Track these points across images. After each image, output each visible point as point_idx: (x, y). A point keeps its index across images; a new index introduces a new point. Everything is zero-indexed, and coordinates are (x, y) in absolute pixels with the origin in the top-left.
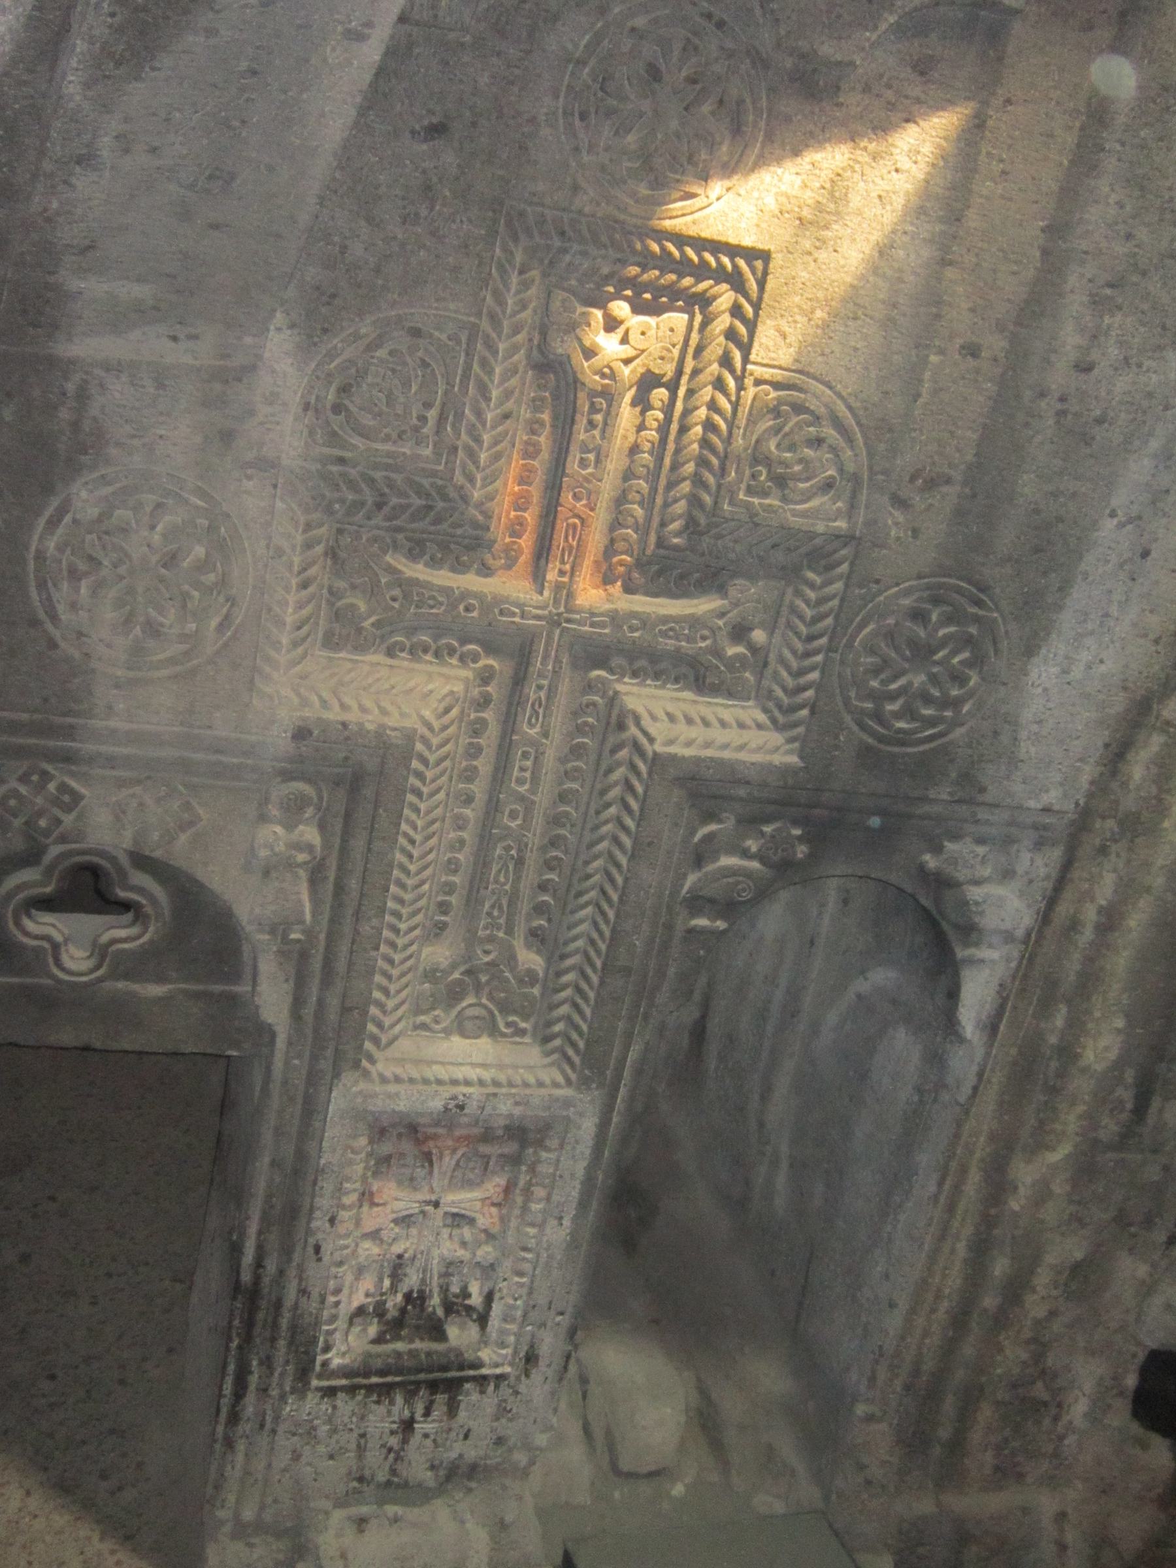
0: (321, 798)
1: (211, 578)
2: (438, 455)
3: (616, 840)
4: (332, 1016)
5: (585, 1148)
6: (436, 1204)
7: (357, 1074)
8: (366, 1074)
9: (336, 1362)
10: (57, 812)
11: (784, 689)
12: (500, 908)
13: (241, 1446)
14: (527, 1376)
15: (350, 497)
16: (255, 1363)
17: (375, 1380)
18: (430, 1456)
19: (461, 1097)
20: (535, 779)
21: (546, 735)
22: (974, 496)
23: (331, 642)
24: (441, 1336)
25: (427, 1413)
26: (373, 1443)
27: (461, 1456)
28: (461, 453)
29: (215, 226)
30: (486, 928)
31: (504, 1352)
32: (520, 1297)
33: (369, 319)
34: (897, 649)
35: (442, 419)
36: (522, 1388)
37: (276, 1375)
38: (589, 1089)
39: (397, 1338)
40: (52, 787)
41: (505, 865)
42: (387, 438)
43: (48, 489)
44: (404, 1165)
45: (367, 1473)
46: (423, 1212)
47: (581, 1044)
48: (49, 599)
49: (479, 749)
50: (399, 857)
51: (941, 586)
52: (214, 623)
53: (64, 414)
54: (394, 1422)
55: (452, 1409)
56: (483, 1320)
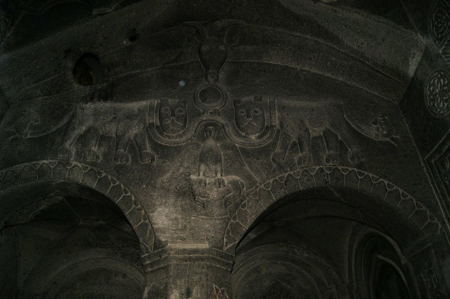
1: (446, 82)
29: (384, 40)
42: (446, 27)
53: (417, 84)
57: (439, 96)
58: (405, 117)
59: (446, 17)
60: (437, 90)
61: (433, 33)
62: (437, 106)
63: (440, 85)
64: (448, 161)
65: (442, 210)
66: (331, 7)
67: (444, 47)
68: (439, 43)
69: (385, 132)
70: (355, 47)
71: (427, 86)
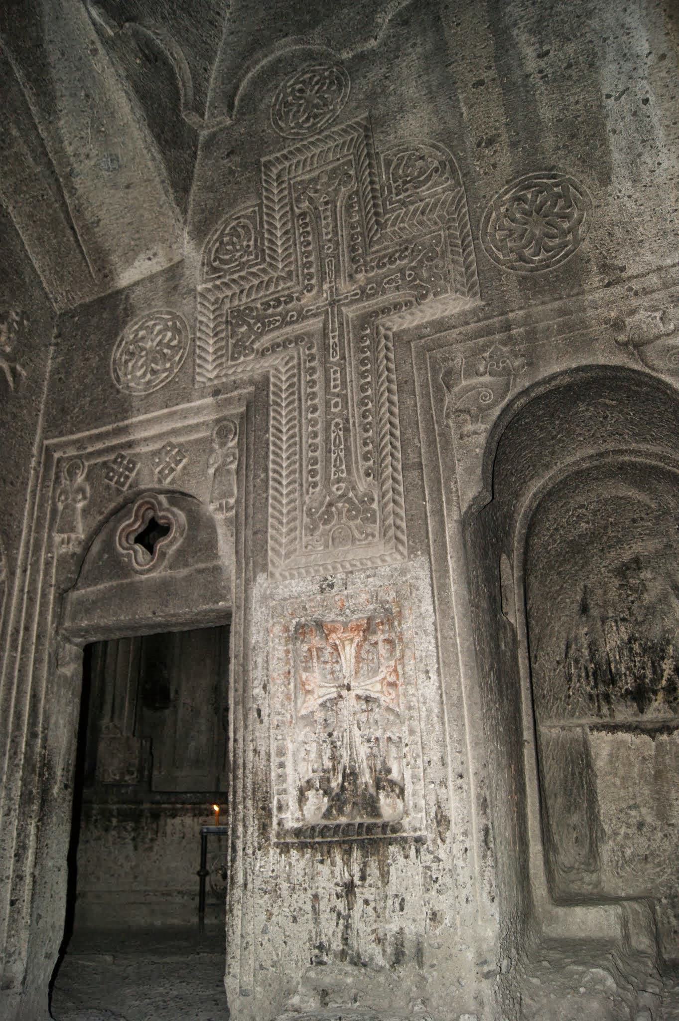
0: (236, 428)
1: (174, 343)
2: (257, 257)
3: (390, 391)
4: (250, 543)
5: (427, 606)
6: (349, 689)
7: (265, 575)
8: (272, 575)
9: (291, 824)
10: (127, 473)
11: (461, 275)
12: (341, 460)
13: (237, 911)
14: (443, 841)
15: (229, 293)
16: (240, 829)
17: (317, 840)
18: (374, 927)
19: (330, 578)
20: (344, 384)
21: (343, 358)
22: (518, 134)
23: (233, 359)
24: (375, 811)
25: (363, 878)
26: (323, 905)
27: (401, 931)
28: (267, 251)
29: (128, 187)
30: (335, 474)
31: (419, 816)
32: (418, 756)
33: (219, 222)
34: (513, 221)
35: (256, 241)
36: (442, 855)
37: (249, 832)
38: (416, 556)
39: (341, 811)
40: (125, 462)
41: (338, 434)
42: (236, 260)
43: (116, 335)
44: (326, 662)
45: (324, 939)
46: (341, 697)
47: (404, 525)
48: (118, 375)
49: (314, 382)
50: (271, 439)
51: (526, 180)
52: (177, 358)
53: (121, 307)
54: (337, 884)
55: (385, 876)
56: (402, 791)
57: (147, 355)
58: (57, 345)
59: (248, 246)
60: (150, 343)
61: (210, 251)
62: (130, 368)
63: (161, 340)
64: (86, 471)
65: (22, 550)
66: (94, 36)
67: (209, 285)
68: (207, 273)
69: (8, 349)
70: (70, 150)
71: (136, 323)
